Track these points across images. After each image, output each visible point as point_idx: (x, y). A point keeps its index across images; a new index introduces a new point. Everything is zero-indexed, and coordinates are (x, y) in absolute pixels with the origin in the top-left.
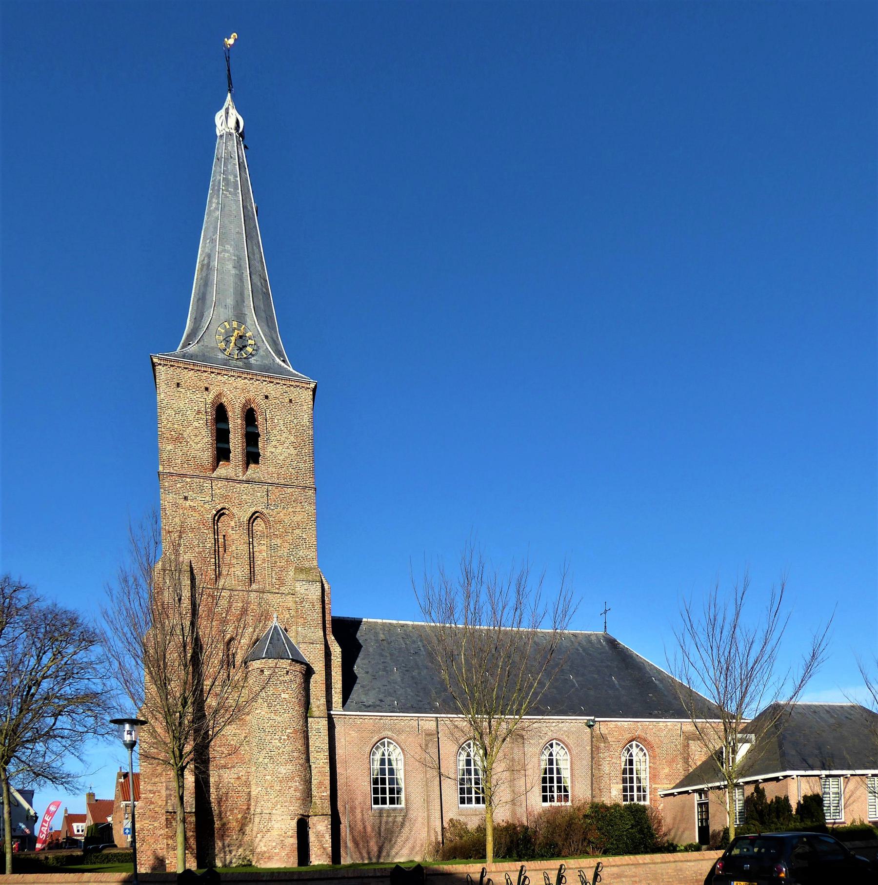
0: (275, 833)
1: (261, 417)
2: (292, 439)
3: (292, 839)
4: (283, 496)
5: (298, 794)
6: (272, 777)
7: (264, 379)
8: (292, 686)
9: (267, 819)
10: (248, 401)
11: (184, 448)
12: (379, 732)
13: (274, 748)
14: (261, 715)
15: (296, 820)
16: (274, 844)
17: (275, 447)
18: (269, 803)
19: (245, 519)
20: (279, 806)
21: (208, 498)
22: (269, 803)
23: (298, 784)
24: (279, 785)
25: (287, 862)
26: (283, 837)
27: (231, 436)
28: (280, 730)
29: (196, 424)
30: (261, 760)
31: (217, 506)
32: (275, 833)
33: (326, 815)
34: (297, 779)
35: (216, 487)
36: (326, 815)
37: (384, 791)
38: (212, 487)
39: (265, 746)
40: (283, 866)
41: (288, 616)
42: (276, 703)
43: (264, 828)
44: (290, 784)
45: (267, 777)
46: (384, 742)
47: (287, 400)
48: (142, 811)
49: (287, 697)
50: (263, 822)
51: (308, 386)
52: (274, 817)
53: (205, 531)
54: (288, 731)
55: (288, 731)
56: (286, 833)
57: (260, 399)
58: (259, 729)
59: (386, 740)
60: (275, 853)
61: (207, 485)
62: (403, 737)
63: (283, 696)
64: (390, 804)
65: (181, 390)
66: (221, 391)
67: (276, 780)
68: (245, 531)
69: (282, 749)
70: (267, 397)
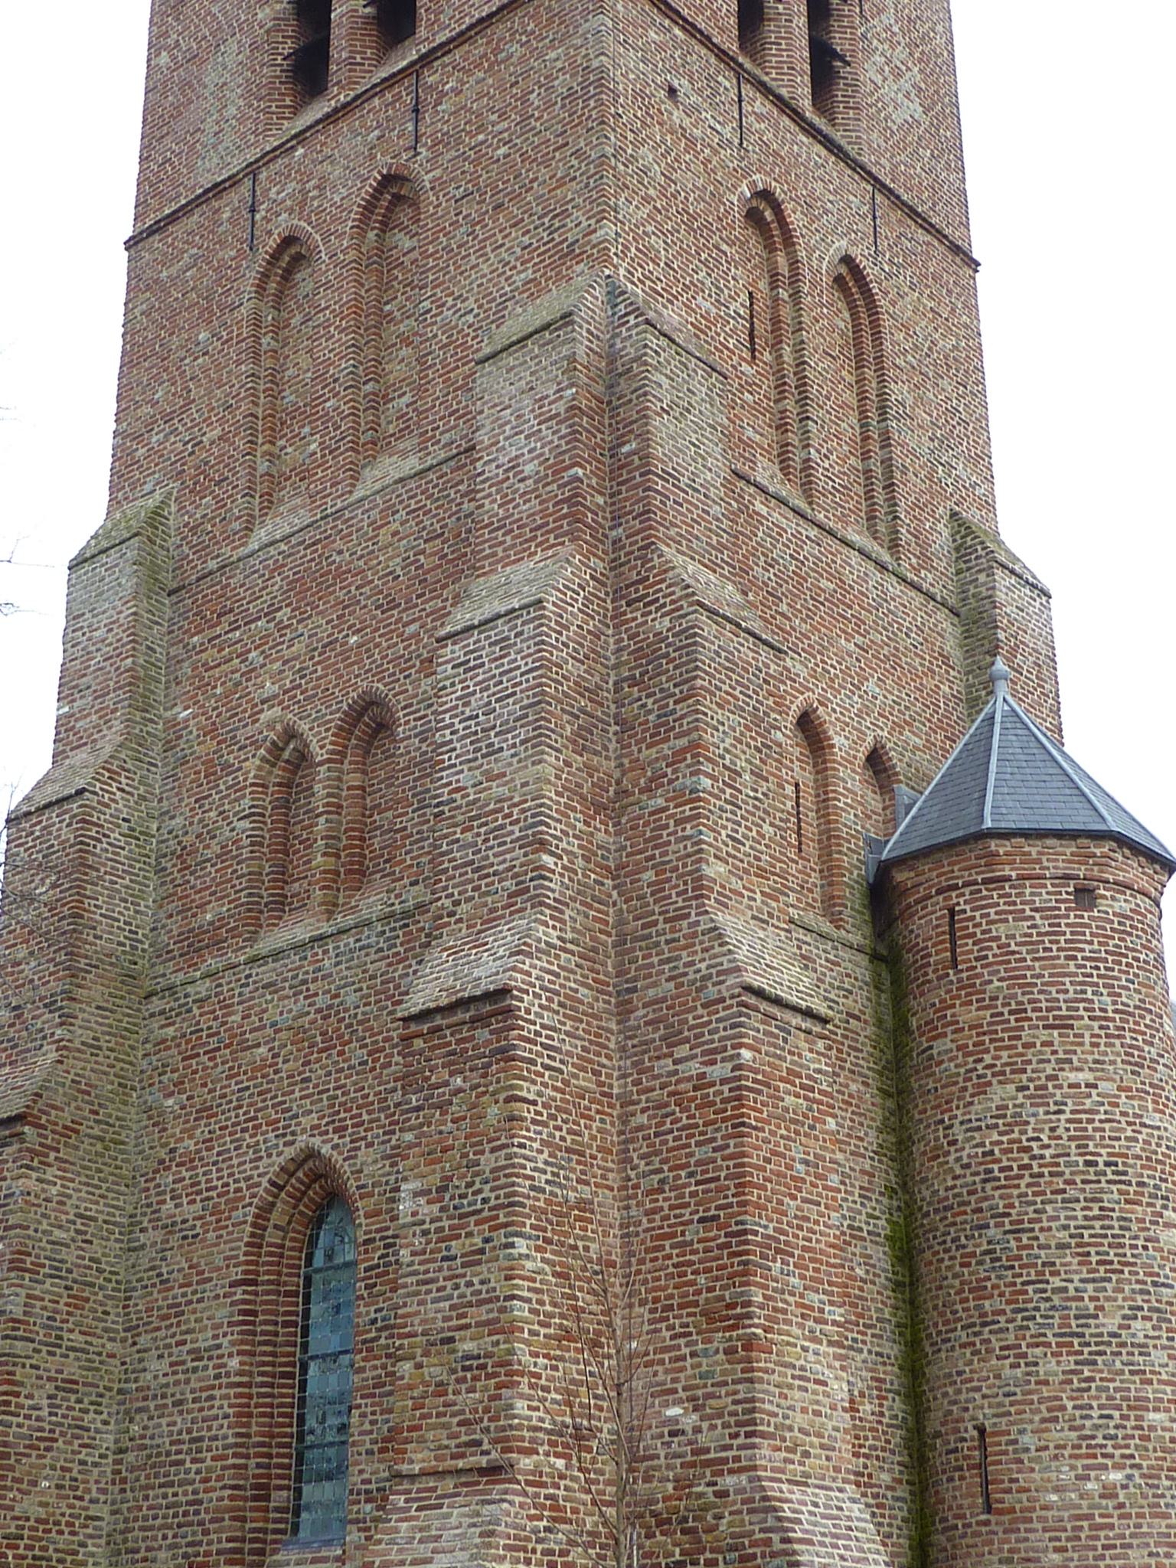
58: (1088, 1163)
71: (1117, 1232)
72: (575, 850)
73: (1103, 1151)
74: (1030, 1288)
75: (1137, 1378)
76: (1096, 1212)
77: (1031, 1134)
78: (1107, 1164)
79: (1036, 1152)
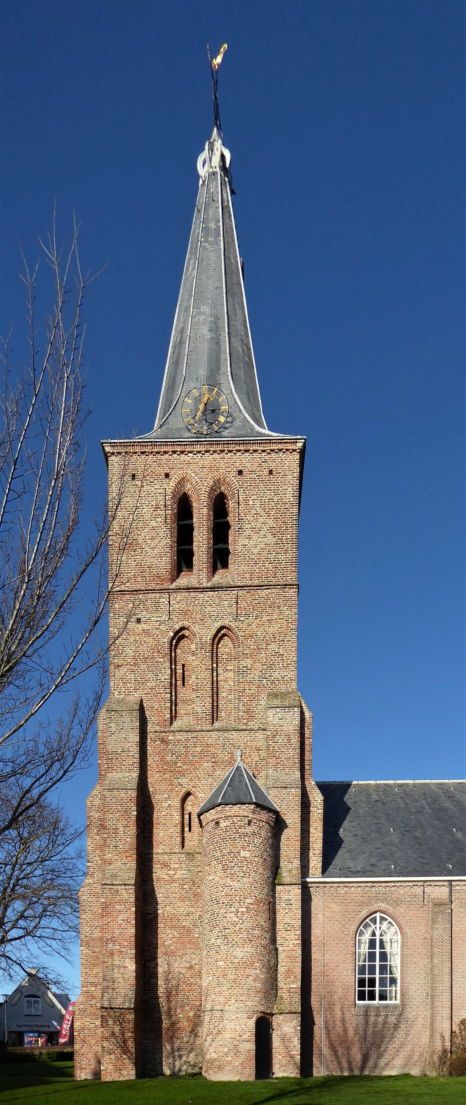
0: (227, 1035)
1: (233, 501)
2: (271, 522)
3: (248, 1043)
4: (256, 602)
5: (259, 985)
6: (225, 963)
7: (238, 448)
8: (256, 841)
9: (218, 1018)
10: (217, 483)
11: (138, 557)
12: (369, 903)
14: (214, 882)
15: (254, 1019)
16: (226, 1050)
17: (249, 538)
18: (221, 996)
19: (209, 637)
20: (233, 1001)
21: (165, 617)
22: (221, 996)
23: (258, 971)
24: (234, 973)
25: (241, 1074)
26: (237, 1041)
27: (195, 533)
28: (237, 900)
29: (153, 523)
30: (212, 941)
31: (175, 626)
32: (227, 1035)
33: (295, 1013)
34: (257, 965)
36: (295, 1013)
37: (372, 983)
38: (169, 602)
39: (218, 922)
40: (236, 1079)
41: (257, 759)
42: (233, 864)
43: (214, 1029)
44: (248, 971)
45: (219, 963)
46: (375, 917)
47: (266, 472)
49: (248, 855)
50: (214, 1021)
51: (294, 447)
52: (226, 1015)
53: (160, 660)
54: (247, 901)
55: (247, 901)
56: (241, 1036)
57: (232, 478)
59: (378, 915)
60: (227, 1061)
62: (402, 910)
63: (243, 854)
64: (380, 999)
66: (185, 475)
67: (230, 966)
68: (208, 654)
69: (239, 925)
70: (240, 472)
72: (98, 859)
75: (217, 954)
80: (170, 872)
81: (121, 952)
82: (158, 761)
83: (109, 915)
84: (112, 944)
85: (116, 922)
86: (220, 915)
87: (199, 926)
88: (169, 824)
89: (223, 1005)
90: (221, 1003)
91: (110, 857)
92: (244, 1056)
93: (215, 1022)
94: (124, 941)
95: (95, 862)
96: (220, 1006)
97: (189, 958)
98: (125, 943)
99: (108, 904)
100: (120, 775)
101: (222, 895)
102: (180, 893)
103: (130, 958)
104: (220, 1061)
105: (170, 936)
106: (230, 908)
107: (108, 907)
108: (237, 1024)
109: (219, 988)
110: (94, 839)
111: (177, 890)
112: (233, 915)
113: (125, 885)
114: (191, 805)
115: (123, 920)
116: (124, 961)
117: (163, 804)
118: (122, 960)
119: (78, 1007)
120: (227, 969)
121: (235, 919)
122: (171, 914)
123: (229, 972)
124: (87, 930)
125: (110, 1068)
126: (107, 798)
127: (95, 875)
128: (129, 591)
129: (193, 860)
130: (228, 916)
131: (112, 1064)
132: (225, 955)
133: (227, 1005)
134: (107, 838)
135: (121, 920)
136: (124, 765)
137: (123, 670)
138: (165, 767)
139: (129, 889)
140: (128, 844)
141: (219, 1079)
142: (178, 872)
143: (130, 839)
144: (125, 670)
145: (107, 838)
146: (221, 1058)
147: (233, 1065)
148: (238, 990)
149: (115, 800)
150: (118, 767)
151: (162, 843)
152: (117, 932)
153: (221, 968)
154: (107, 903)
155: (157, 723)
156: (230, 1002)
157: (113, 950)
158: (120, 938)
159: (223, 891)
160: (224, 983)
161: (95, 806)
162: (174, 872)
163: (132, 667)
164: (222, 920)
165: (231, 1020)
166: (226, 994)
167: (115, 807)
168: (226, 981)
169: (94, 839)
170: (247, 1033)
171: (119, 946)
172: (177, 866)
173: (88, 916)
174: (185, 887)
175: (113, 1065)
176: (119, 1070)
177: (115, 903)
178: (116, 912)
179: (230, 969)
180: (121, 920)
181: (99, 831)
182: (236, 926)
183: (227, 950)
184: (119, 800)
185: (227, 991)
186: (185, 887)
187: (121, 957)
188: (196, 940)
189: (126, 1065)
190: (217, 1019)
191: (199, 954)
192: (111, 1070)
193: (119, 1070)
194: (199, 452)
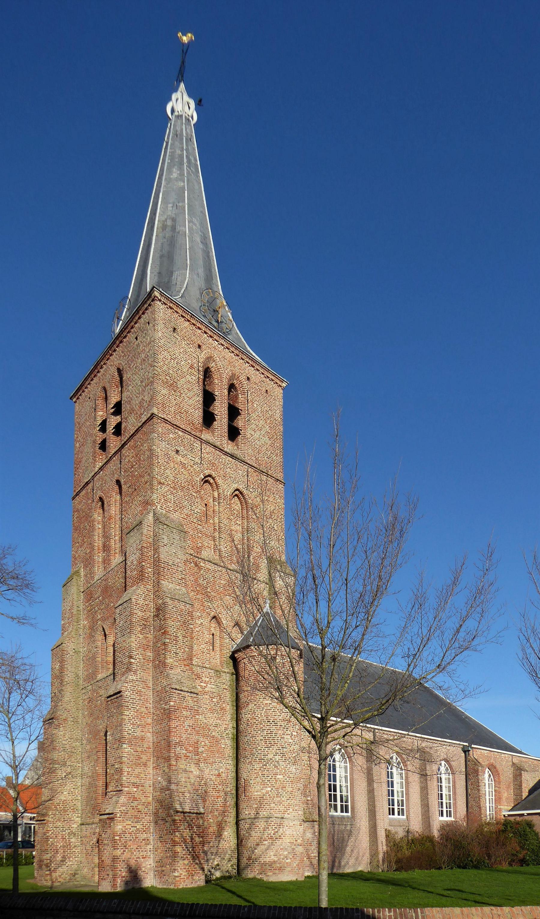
0: (287, 840)
1: (243, 396)
3: (301, 847)
6: (284, 777)
7: (248, 360)
9: (279, 824)
11: (177, 398)
13: (286, 745)
14: (271, 707)
16: (286, 853)
18: (281, 806)
20: (291, 810)
21: (197, 460)
22: (281, 806)
24: (290, 787)
25: (298, 874)
26: (294, 845)
28: (291, 725)
30: (270, 756)
31: (205, 472)
32: (287, 840)
35: (205, 451)
38: (201, 450)
39: (276, 741)
40: (294, 879)
45: (278, 776)
47: (264, 390)
48: (124, 808)
50: (274, 827)
52: (286, 822)
53: (194, 494)
56: (297, 841)
57: (243, 378)
58: (268, 722)
60: (287, 863)
61: (197, 445)
65: (177, 337)
66: (212, 355)
67: (288, 780)
69: (293, 746)
71: (274, 736)
72: (141, 657)
73: (272, 719)
74: (254, 749)
75: (276, 768)
76: (269, 732)
77: (256, 715)
78: (272, 721)
79: (257, 719)
80: (202, 684)
81: (187, 756)
82: (193, 581)
83: (177, 719)
84: (179, 748)
85: (183, 727)
86: (278, 735)
87: (225, 738)
88: (201, 640)
89: (283, 814)
90: (281, 811)
91: (171, 662)
92: (299, 858)
93: (275, 828)
94: (190, 747)
95: (138, 659)
96: (280, 814)
97: (218, 766)
98: (191, 748)
99: (176, 708)
100: (171, 586)
101: (279, 718)
102: (210, 705)
103: (195, 764)
104: (281, 863)
105: (203, 743)
106: (286, 730)
107: (176, 711)
108: (294, 830)
109: (279, 798)
110: (138, 637)
111: (208, 702)
112: (289, 737)
113: (191, 692)
114: (214, 628)
115: (189, 726)
116: (190, 766)
117: (197, 621)
118: (188, 764)
119: (120, 808)
120: (285, 782)
121: (291, 741)
122: (203, 723)
123: (287, 785)
124: (130, 727)
125: (184, 874)
126: (169, 605)
127: (138, 673)
128: (171, 423)
129: (220, 677)
130: (285, 737)
131: (185, 870)
132: (283, 770)
133: (286, 813)
134: (169, 643)
135: (188, 726)
136: (174, 578)
137: (165, 489)
138: (198, 589)
139: (195, 697)
140: (187, 654)
141: (280, 880)
142: (209, 685)
143: (188, 650)
144: (166, 489)
145: (169, 643)
146: (281, 860)
147: (291, 866)
148: (294, 801)
149: (176, 609)
150: (169, 578)
151: (195, 656)
152: (184, 737)
153: (280, 781)
154: (175, 707)
155: (192, 547)
156: (288, 811)
157: (180, 753)
158: (186, 743)
159: (281, 716)
160: (283, 794)
161: (139, 604)
162: (205, 685)
163: (172, 490)
164: (280, 740)
165: (290, 826)
166: (286, 804)
167: (175, 616)
168: (284, 792)
169: (138, 637)
170: (300, 838)
171: (186, 750)
172: (207, 680)
173: (130, 713)
174: (214, 700)
175: (186, 871)
176: (192, 876)
177: (183, 708)
178: (183, 717)
179: (287, 783)
180: (188, 726)
181: (142, 630)
182: (291, 747)
183: (285, 766)
184: (179, 610)
185: (286, 801)
186: (214, 700)
187: (187, 762)
188: (222, 750)
189: (197, 871)
190: (277, 825)
191: (225, 763)
192: (184, 876)
193: (192, 876)
194: (223, 345)
